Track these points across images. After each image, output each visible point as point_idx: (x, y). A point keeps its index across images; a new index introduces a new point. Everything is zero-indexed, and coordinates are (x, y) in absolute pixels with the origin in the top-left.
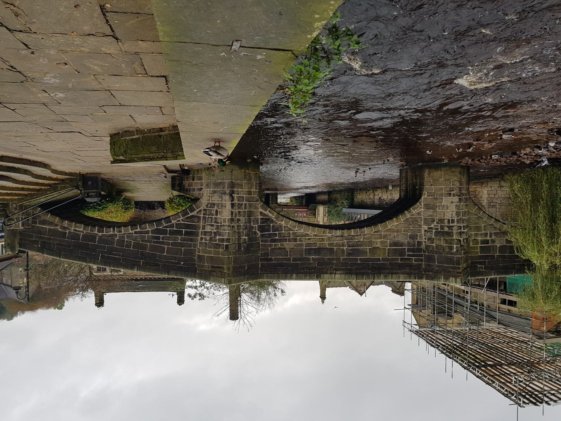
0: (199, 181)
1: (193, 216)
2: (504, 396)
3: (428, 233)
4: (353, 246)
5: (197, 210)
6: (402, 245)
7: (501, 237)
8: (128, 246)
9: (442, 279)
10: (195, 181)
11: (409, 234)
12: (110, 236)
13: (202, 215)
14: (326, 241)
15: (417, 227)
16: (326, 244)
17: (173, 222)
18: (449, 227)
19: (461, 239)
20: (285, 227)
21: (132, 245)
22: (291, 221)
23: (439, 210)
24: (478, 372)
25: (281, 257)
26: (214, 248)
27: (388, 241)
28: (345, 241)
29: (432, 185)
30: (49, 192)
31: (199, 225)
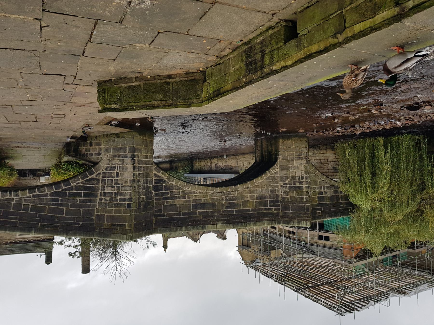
2: (329, 310)
4: (230, 201)
6: (265, 198)
7: (330, 189)
8: (26, 208)
11: (270, 189)
12: (6, 200)
13: (101, 178)
14: (209, 197)
16: (209, 199)
17: (72, 184)
18: (300, 183)
19: (309, 191)
20: (175, 186)
21: (30, 208)
24: (306, 293)
26: (115, 208)
27: (256, 195)
28: (223, 196)
31: (98, 187)
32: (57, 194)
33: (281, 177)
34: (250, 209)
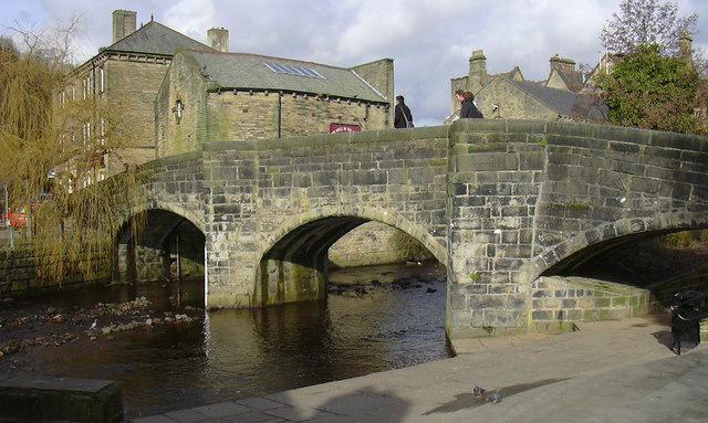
1: (550, 244)
10: (554, 310)
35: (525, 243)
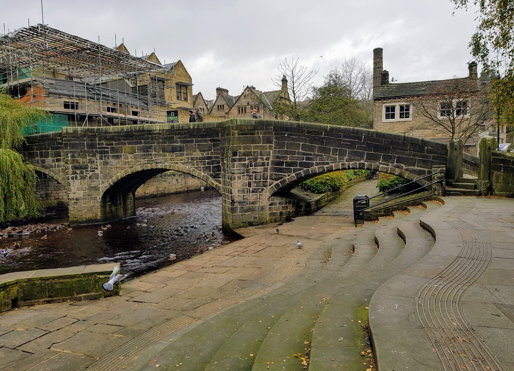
0: (274, 211)
1: (277, 180)
3: (95, 167)
4: (148, 154)
5: (273, 185)
6: (113, 156)
7: (49, 164)
8: (335, 151)
9: (79, 130)
10: (278, 212)
11: (109, 166)
13: (269, 181)
14: (168, 158)
15: (103, 172)
16: (168, 156)
17: (294, 175)
20: (201, 170)
21: (331, 151)
22: (196, 176)
23: (85, 186)
25: (203, 143)
27: (123, 160)
28: (154, 159)
29: (93, 206)
30: (394, 207)
31: (271, 172)
32: (308, 165)
33: (98, 178)
34: (127, 145)
35: (265, 178)
